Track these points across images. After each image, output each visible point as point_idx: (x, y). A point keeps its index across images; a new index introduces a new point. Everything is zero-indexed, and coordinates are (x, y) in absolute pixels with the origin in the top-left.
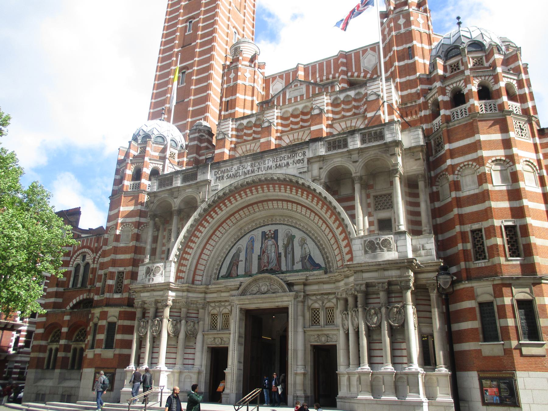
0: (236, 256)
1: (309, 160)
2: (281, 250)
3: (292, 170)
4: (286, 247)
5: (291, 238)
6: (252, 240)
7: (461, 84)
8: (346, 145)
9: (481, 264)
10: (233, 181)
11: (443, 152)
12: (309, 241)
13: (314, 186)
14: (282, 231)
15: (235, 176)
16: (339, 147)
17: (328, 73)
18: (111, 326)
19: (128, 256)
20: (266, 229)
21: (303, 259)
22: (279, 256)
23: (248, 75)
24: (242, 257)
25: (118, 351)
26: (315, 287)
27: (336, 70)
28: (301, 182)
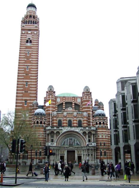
0: (65, 142)
1: (80, 130)
2: (73, 142)
3: (77, 131)
4: (74, 141)
5: (75, 140)
6: (68, 139)
7: (101, 122)
8: (86, 128)
9: (101, 147)
10: (67, 130)
12: (78, 141)
13: (81, 134)
14: (73, 139)
15: (67, 129)
17: (70, 100)
18: (41, 152)
19: (42, 139)
20: (70, 138)
21: (77, 144)
23: (54, 97)
24: (66, 142)
25: (42, 156)
26: (79, 148)
27: (72, 100)
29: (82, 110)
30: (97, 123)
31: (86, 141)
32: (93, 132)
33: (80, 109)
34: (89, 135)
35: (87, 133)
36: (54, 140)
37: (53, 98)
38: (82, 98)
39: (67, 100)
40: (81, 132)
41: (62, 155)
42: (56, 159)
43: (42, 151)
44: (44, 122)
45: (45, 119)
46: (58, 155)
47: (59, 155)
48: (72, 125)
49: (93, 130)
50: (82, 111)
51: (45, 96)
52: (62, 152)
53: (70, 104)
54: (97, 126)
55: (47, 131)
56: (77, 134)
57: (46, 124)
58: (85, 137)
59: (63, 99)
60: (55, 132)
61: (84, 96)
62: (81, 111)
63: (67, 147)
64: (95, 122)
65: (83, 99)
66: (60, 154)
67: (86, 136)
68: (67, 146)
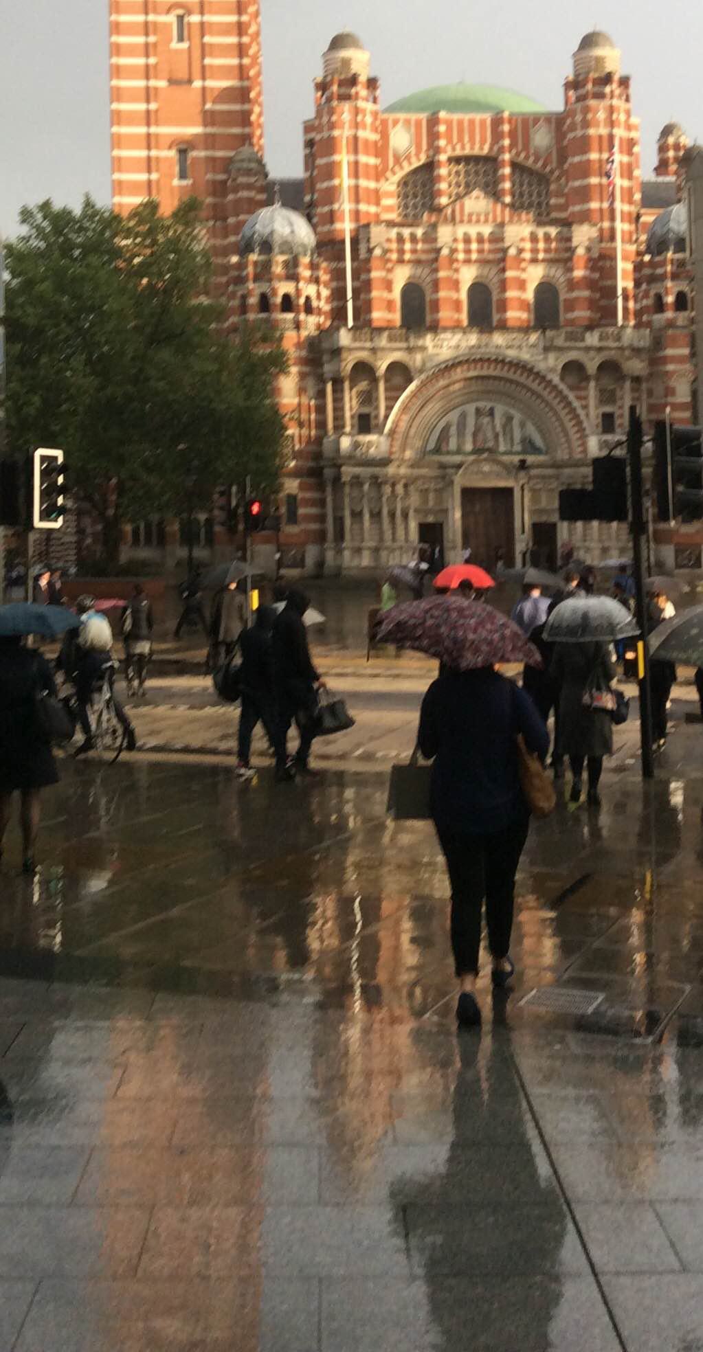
0: (446, 430)
2: (499, 428)
4: (504, 427)
5: (509, 419)
6: (463, 416)
11: (662, 354)
13: (549, 377)
14: (500, 410)
16: (576, 340)
17: (483, 142)
18: (292, 499)
20: (481, 404)
22: (496, 436)
24: (453, 430)
25: (303, 526)
28: (535, 370)
29: (563, 208)
30: (659, 299)
31: (585, 424)
32: (636, 366)
33: (553, 201)
34: (608, 383)
35: (592, 367)
36: (373, 422)
37: (364, 127)
38: (558, 122)
39: (461, 139)
40: (551, 364)
41: (431, 519)
42: (394, 539)
43: (300, 496)
44: (308, 298)
45: (316, 281)
46: (405, 516)
47: (411, 513)
48: (496, 317)
49: (636, 351)
50: (563, 215)
51: (310, 113)
52: (431, 496)
53: (482, 168)
54: (659, 318)
55: (325, 358)
56: (522, 380)
57: (319, 312)
58: (579, 398)
59: (433, 136)
60: (382, 366)
61: (579, 105)
62: (554, 215)
63: (459, 466)
64: (646, 295)
65: (573, 128)
66: (416, 511)
67: (586, 388)
68: (457, 459)
